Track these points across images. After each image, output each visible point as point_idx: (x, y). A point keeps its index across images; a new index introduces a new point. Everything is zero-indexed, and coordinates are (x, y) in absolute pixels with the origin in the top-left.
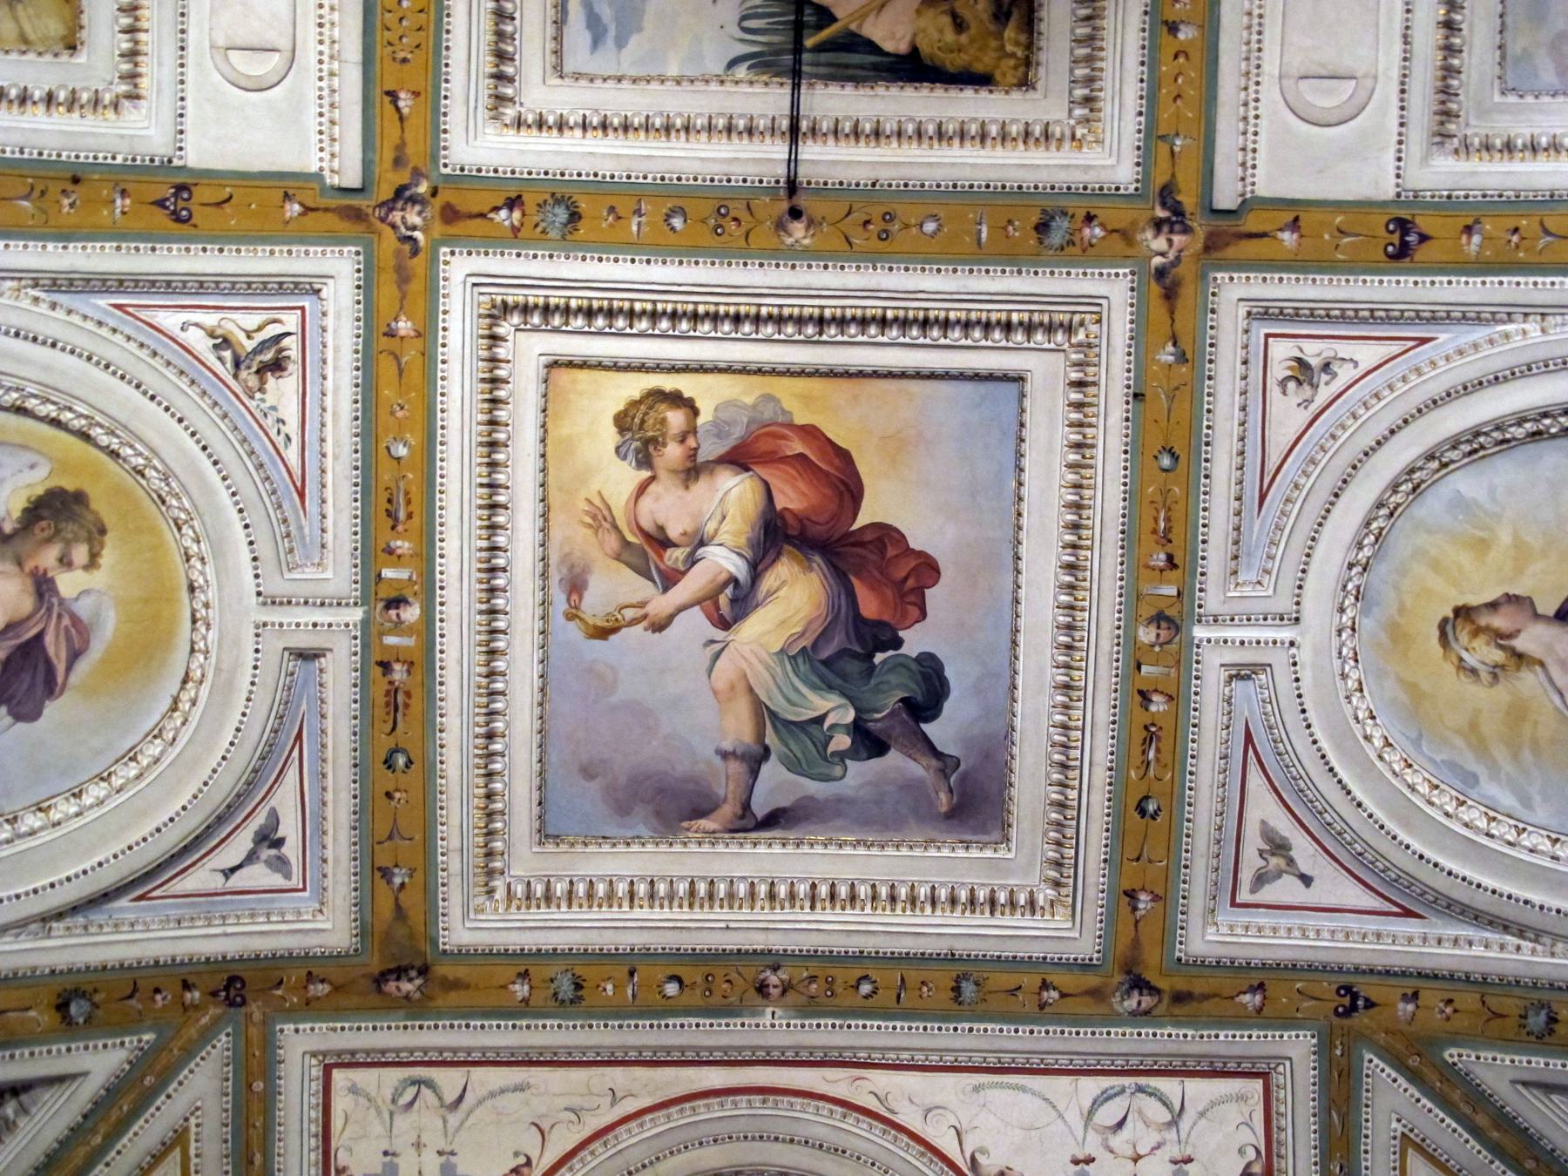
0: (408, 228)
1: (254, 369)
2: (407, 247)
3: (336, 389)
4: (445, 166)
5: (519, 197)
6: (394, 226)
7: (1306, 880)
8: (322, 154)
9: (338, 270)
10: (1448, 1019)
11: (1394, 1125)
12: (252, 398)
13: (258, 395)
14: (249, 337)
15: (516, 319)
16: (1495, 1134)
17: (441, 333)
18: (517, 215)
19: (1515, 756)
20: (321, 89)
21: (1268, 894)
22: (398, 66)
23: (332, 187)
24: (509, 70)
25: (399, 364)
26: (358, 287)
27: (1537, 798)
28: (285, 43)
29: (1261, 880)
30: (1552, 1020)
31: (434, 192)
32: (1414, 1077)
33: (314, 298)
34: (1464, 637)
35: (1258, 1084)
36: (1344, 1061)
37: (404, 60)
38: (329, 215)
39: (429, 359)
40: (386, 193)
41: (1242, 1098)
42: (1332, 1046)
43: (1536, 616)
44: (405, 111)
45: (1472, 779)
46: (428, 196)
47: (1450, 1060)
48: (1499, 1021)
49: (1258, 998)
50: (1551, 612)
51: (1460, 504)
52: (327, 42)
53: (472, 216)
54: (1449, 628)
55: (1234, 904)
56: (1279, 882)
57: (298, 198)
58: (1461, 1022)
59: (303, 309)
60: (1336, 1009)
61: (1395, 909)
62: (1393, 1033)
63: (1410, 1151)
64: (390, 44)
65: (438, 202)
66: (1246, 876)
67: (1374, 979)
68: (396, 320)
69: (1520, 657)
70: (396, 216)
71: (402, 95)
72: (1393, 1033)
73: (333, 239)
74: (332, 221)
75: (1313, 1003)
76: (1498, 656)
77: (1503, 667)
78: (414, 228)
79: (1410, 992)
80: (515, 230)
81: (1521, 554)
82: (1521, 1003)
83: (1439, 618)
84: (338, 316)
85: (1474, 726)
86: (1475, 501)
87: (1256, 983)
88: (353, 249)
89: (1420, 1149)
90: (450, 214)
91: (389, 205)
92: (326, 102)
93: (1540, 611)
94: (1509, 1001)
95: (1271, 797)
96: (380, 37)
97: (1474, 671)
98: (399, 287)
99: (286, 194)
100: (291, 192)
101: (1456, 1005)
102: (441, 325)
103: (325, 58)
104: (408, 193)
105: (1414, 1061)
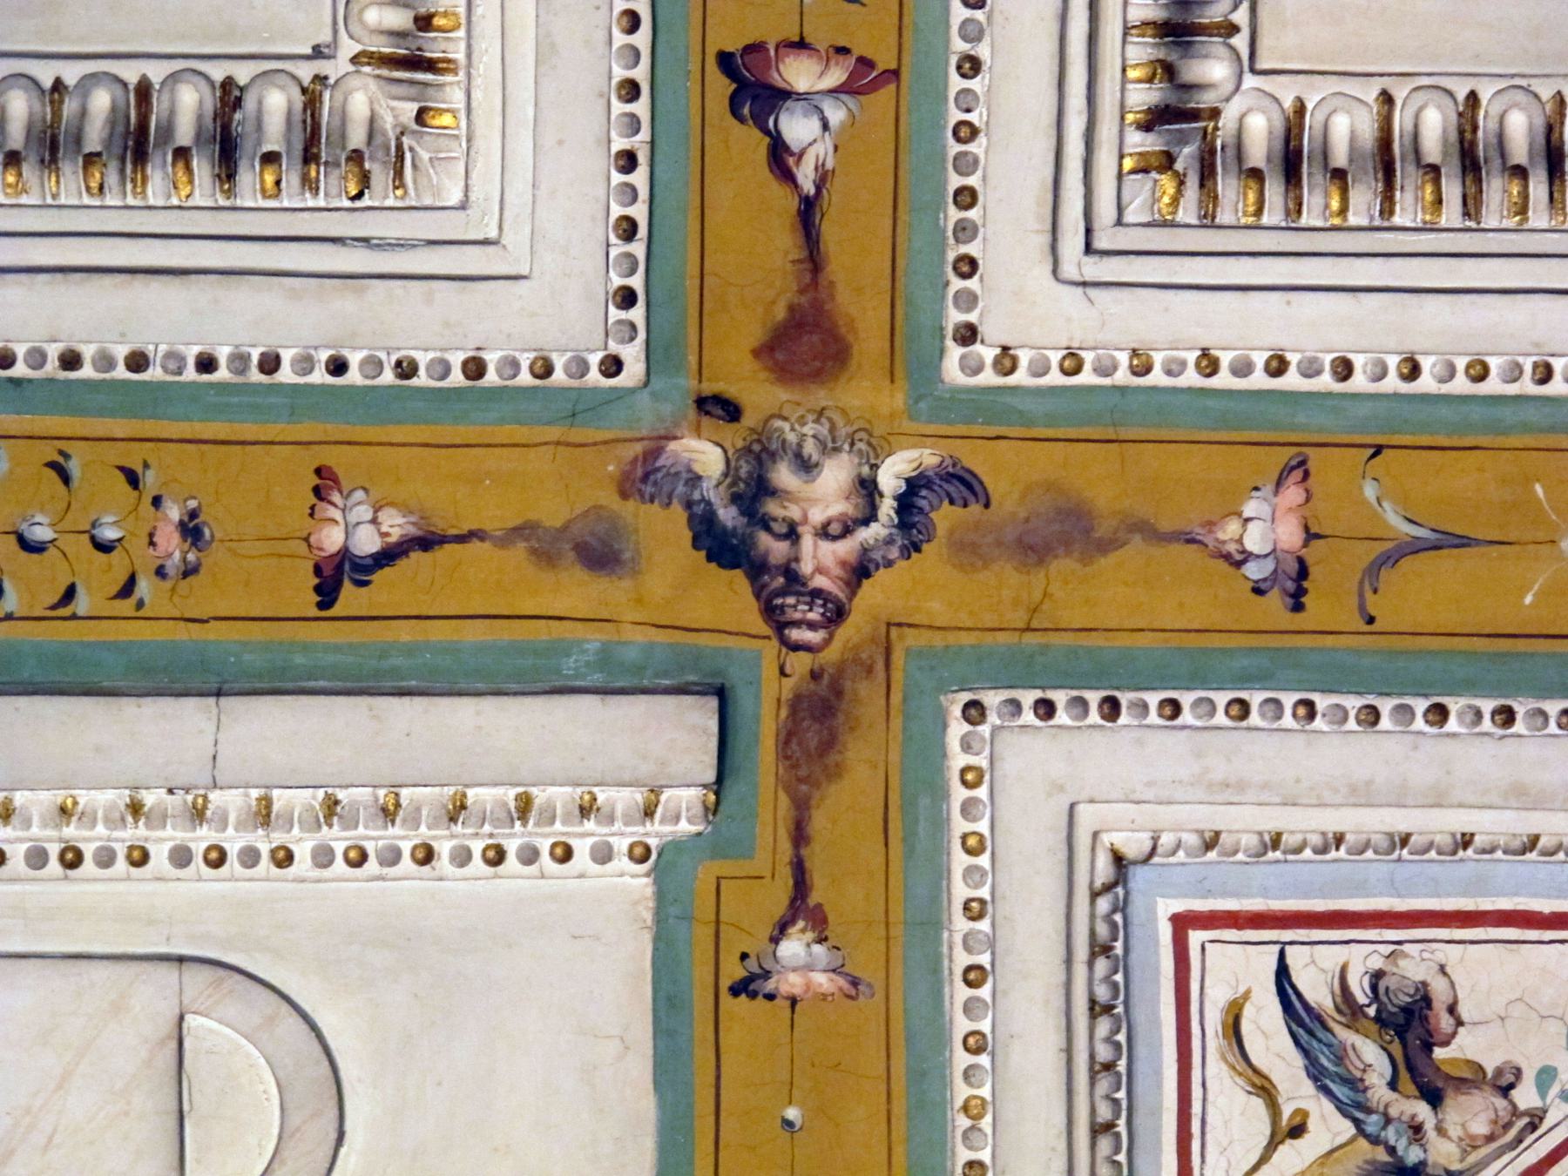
0: (869, 518)
1: (1422, 1110)
2: (945, 517)
3: (1522, 796)
4: (613, 366)
5: (725, 61)
6: (860, 571)
8: (582, 848)
9: (1045, 794)
12: (1535, 1120)
13: (1525, 1096)
14: (1297, 1131)
15: (1212, 68)
17: (1292, 380)
18: (799, 74)
20: (323, 857)
22: (215, 557)
23: (712, 811)
24: (188, 106)
25: (1415, 548)
26: (1111, 708)
28: (154, 994)
31: (719, 408)
33: (1139, 878)
37: (191, 530)
38: (819, 822)
39: (1395, 431)
40: (730, 598)
44: (396, 525)
46: (735, 435)
52: (136, 833)
53: (813, 257)
57: (755, 944)
59: (1182, 923)
64: (128, 589)
65: (760, 394)
68: (1238, 560)
70: (820, 560)
71: (332, 539)
73: (911, 818)
74: (844, 810)
78: (867, 488)
80: (865, 78)
84: (1231, 790)
88: (957, 728)
90: (806, 342)
91: (777, 589)
92: (374, 838)
96: (99, 629)
98: (1106, 546)
99: (742, 988)
100: (734, 971)
102: (1259, 380)
103: (200, 839)
104: (728, 515)
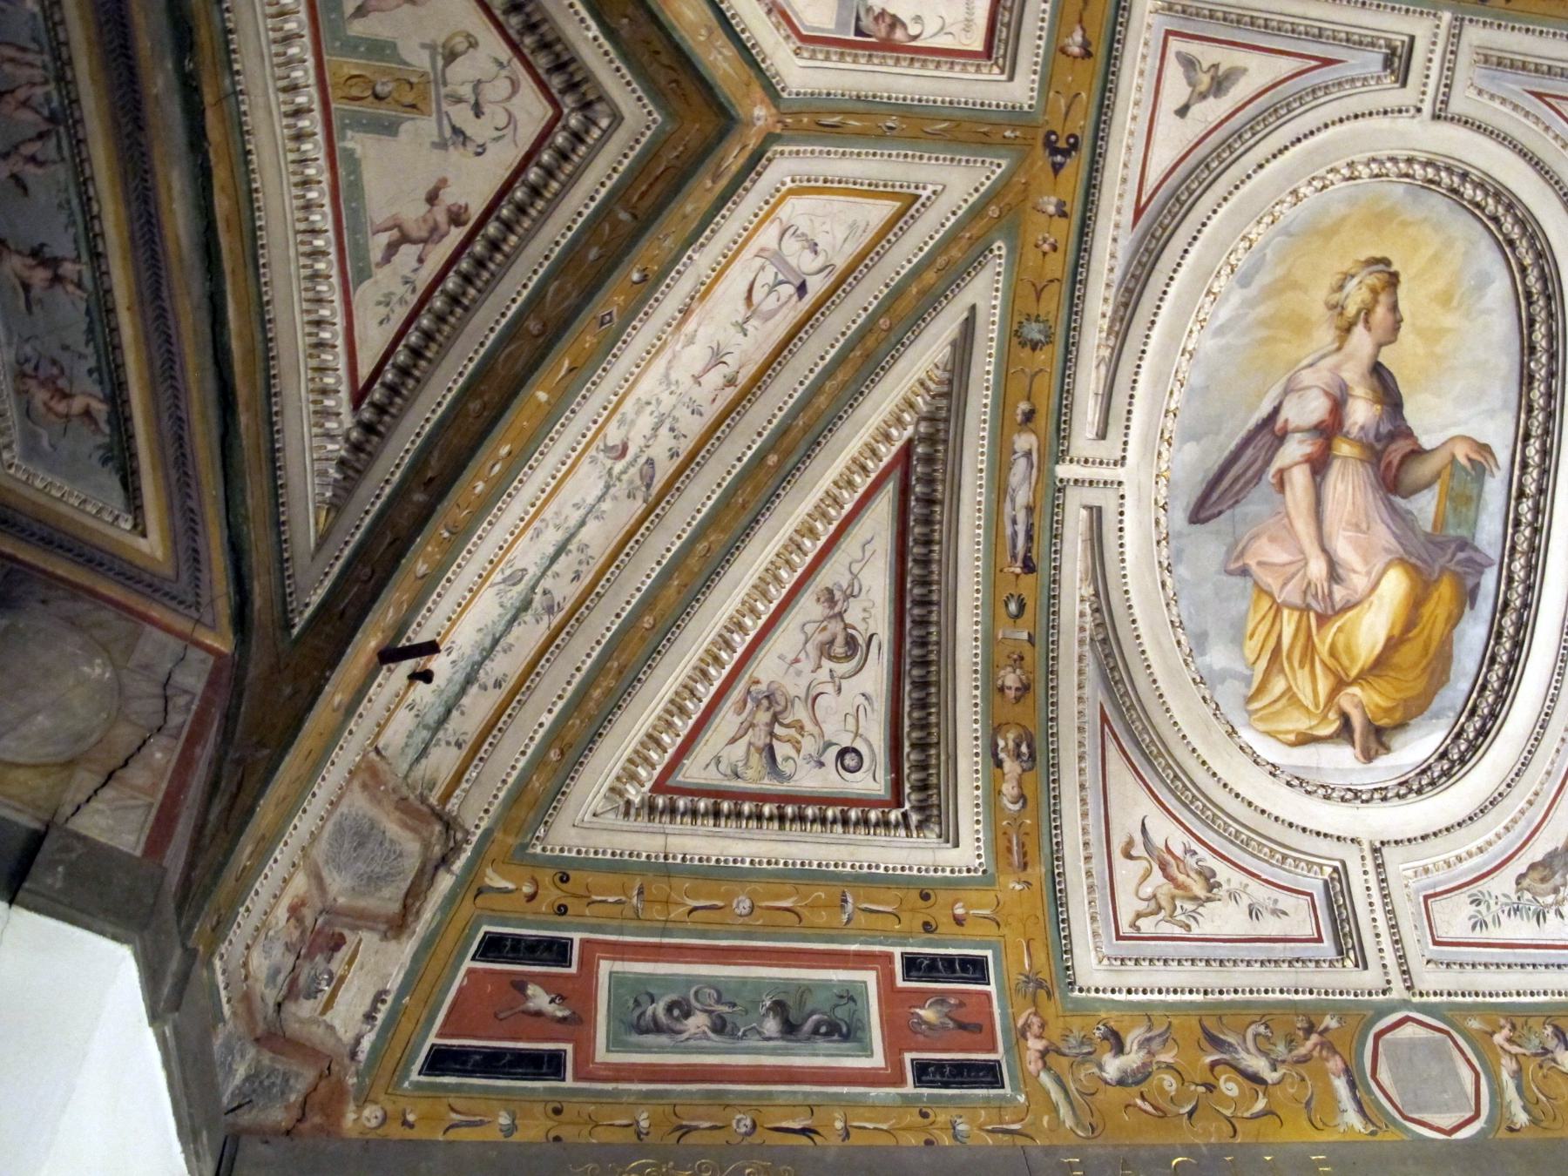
7: (1182, 112)
10: (1037, 246)
11: (930, 188)
16: (914, 290)
19: (1263, 323)
21: (1174, 70)
27: (1222, 341)
29: (1189, 63)
30: (1035, 346)
32: (976, 211)
34: (1372, 280)
35: (978, 45)
36: (997, 138)
41: (968, 26)
42: (1014, 128)
43: (1379, 346)
45: (1245, 282)
47: (994, 247)
48: (1033, 296)
49: (1076, 50)
50: (1386, 357)
51: (1483, 283)
54: (1381, 267)
55: (1168, 33)
56: (1184, 82)
58: (1032, 258)
60: (1054, 133)
61: (1144, 199)
62: (1025, 190)
63: (898, 204)
66: (1193, 48)
67: (1083, 174)
69: (1347, 329)
72: (1025, 190)
75: (1063, 109)
76: (1351, 310)
77: (1341, 314)
79: (1067, 209)
81: (1433, 335)
82: (1051, 317)
83: (1391, 258)
85: (1295, 286)
86: (1480, 298)
87: (1091, 49)
89: (899, 215)
93: (1384, 350)
94: (1053, 306)
95: (1266, 80)
97: (1341, 288)
101: (1052, 255)
105: (993, 211)
